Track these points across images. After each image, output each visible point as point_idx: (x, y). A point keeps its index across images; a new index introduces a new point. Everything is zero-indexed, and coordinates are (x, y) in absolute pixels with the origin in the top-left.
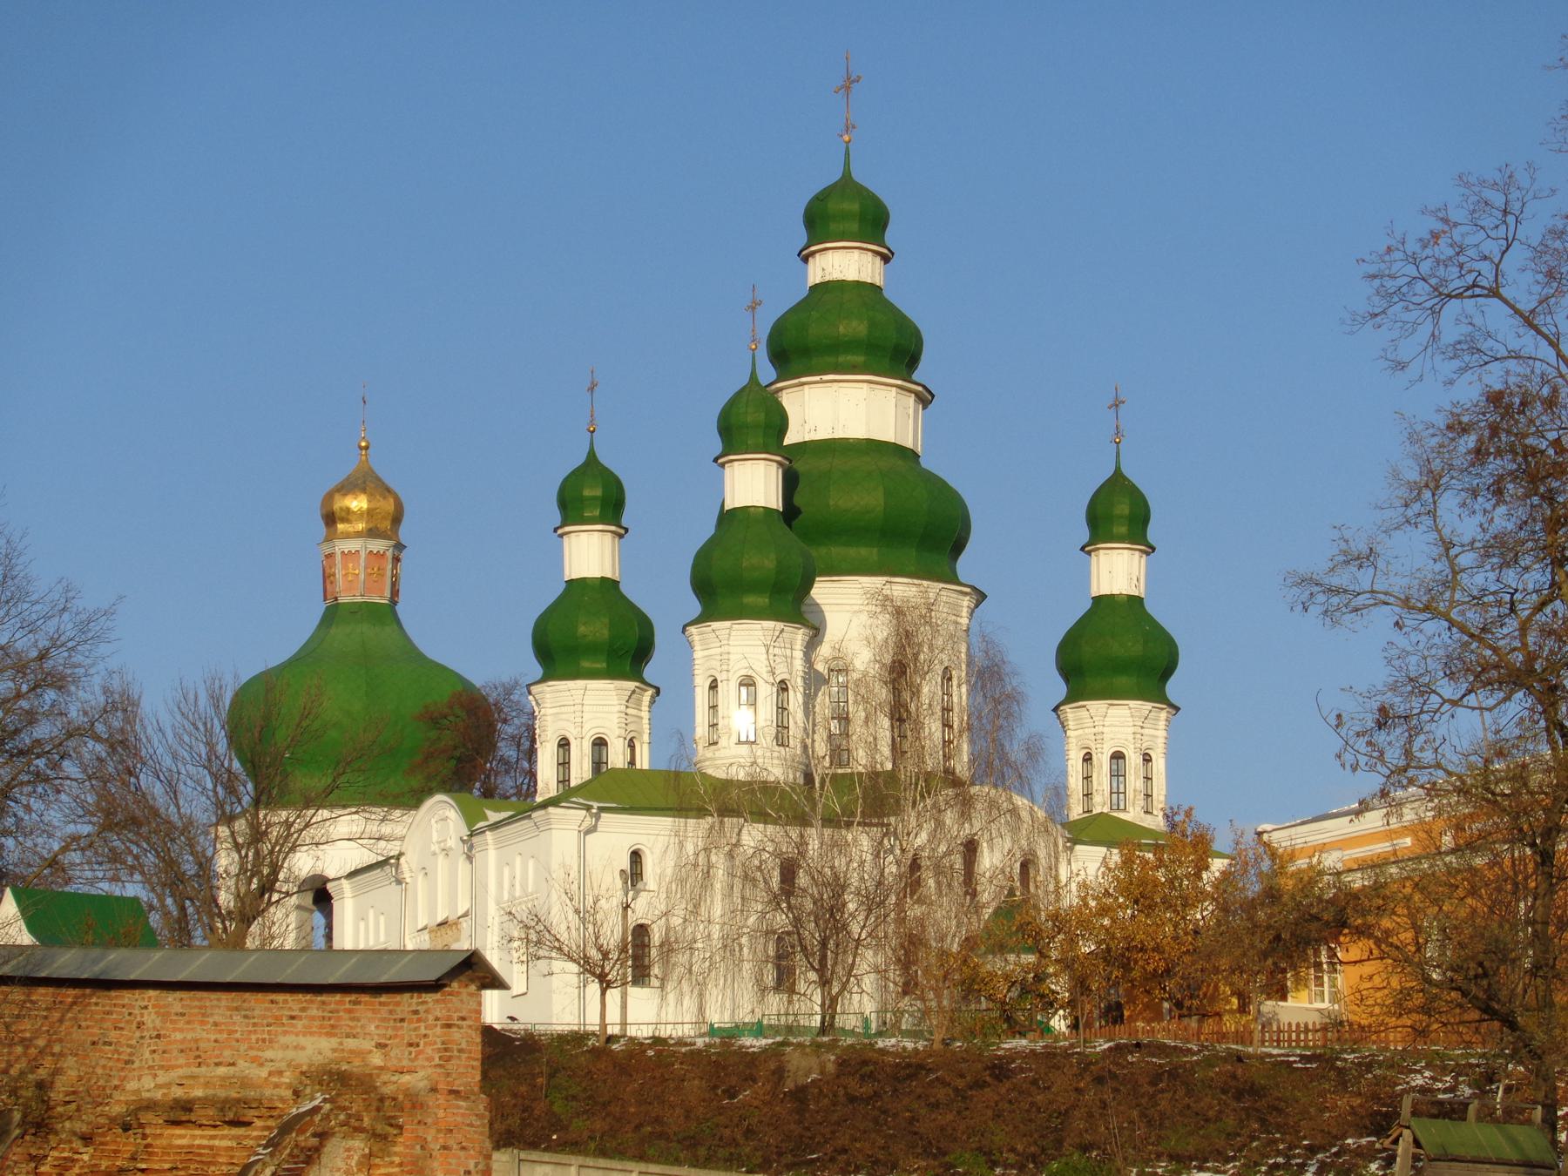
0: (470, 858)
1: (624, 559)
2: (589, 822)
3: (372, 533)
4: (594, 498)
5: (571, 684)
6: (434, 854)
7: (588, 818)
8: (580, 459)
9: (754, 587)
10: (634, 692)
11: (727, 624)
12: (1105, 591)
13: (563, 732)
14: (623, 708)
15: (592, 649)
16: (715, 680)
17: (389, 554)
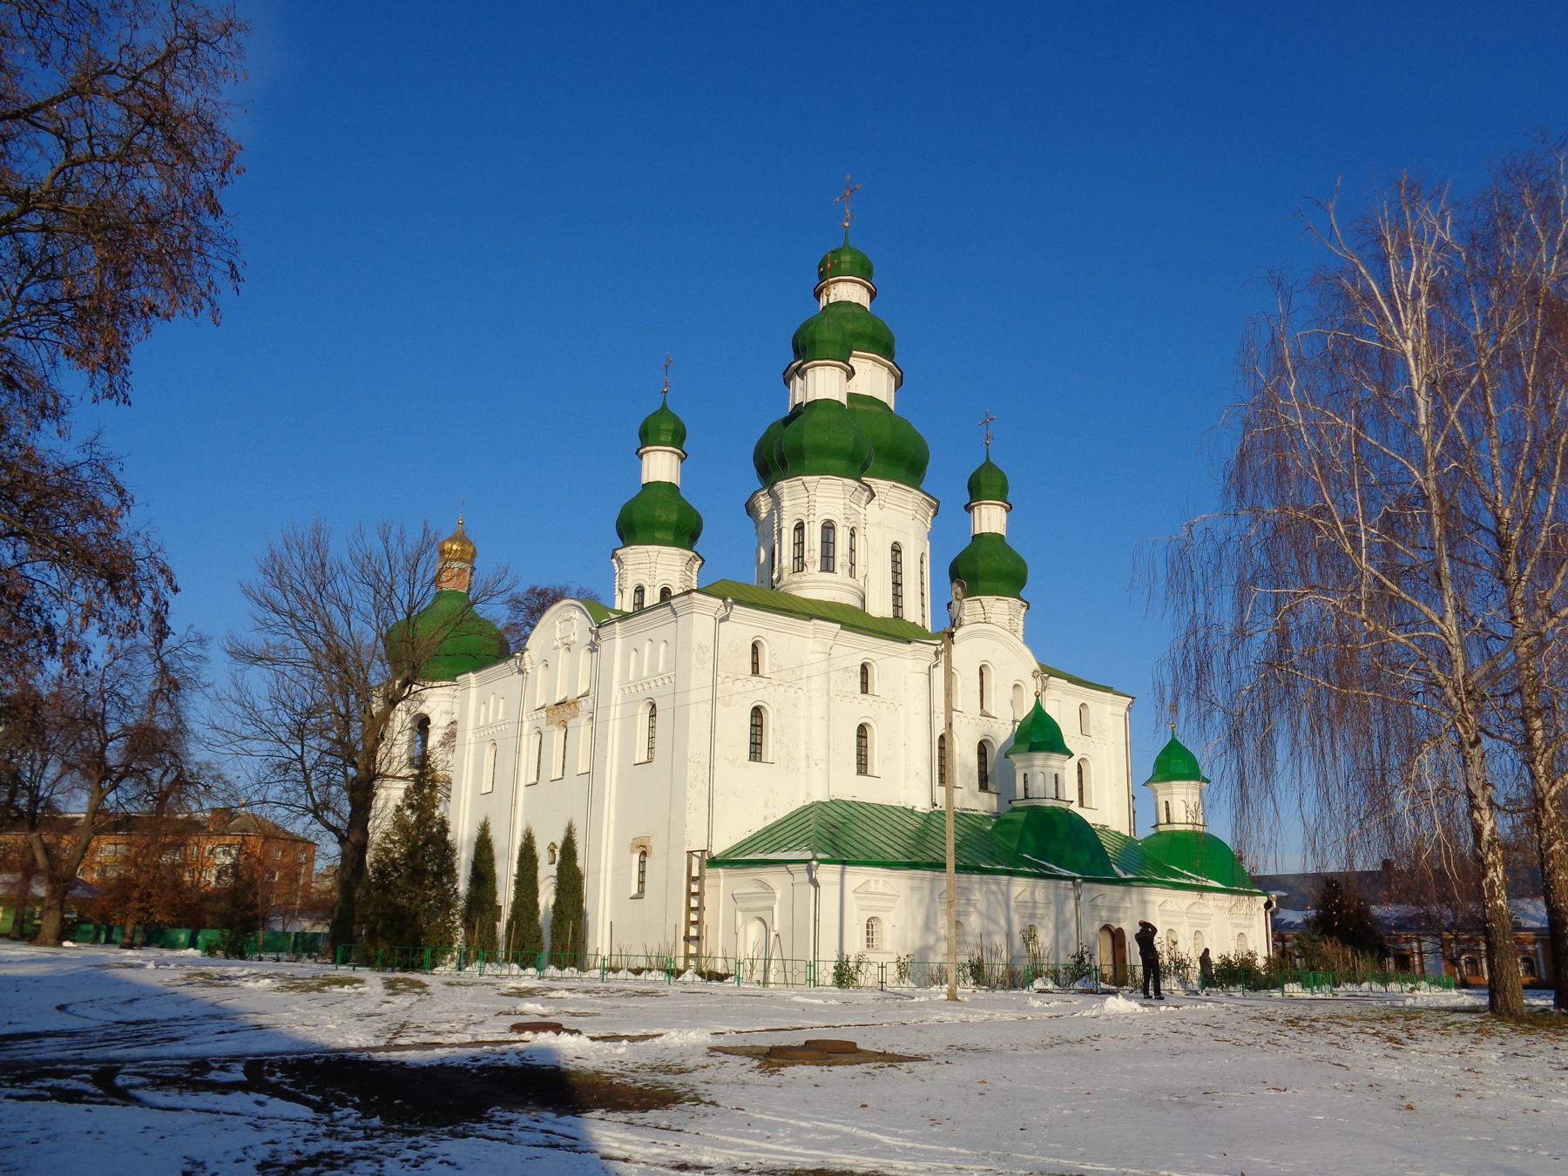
0: (593, 647)
1: (684, 473)
2: (722, 612)
3: (460, 559)
4: (668, 430)
5: (649, 548)
6: (557, 648)
7: (723, 608)
8: (657, 407)
9: (835, 453)
10: (690, 559)
11: (817, 478)
12: (985, 530)
13: (640, 582)
14: (684, 569)
15: (664, 526)
16: (803, 523)
17: (469, 570)
